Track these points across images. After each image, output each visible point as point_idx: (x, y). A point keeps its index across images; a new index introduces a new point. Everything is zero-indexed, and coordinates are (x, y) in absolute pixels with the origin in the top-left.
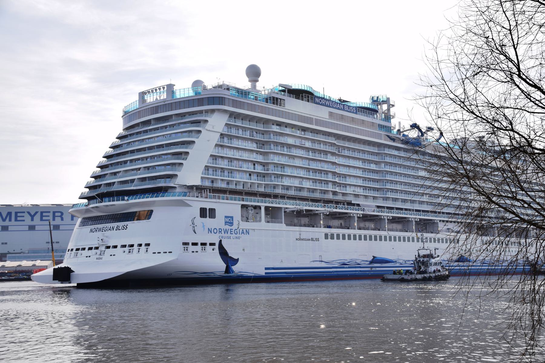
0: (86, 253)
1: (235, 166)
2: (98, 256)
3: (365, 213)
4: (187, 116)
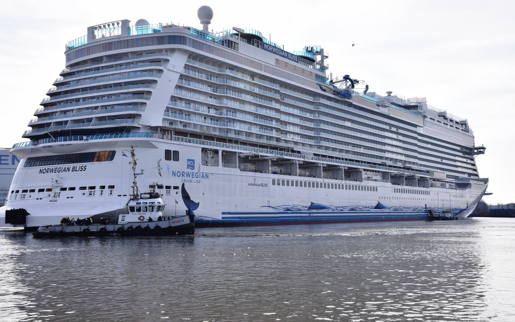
0: (36, 194)
1: (192, 108)
2: (51, 199)
3: (306, 160)
4: (144, 54)
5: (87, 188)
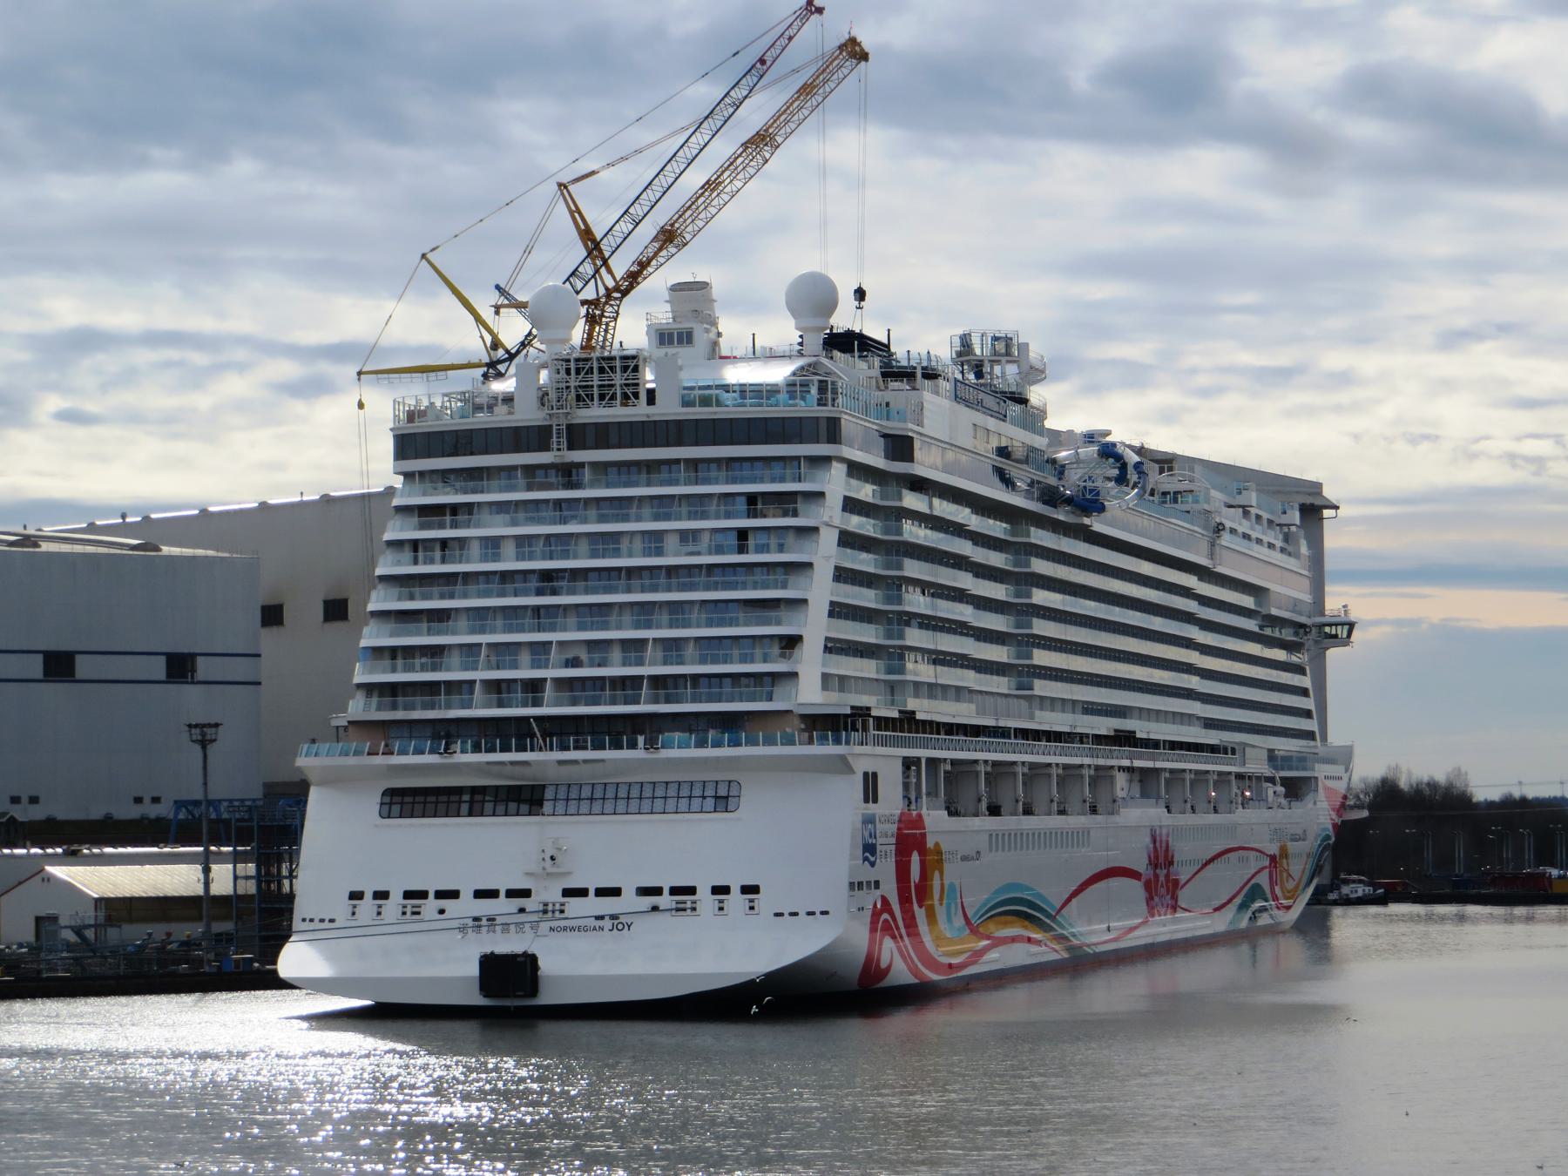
5: (666, 891)
